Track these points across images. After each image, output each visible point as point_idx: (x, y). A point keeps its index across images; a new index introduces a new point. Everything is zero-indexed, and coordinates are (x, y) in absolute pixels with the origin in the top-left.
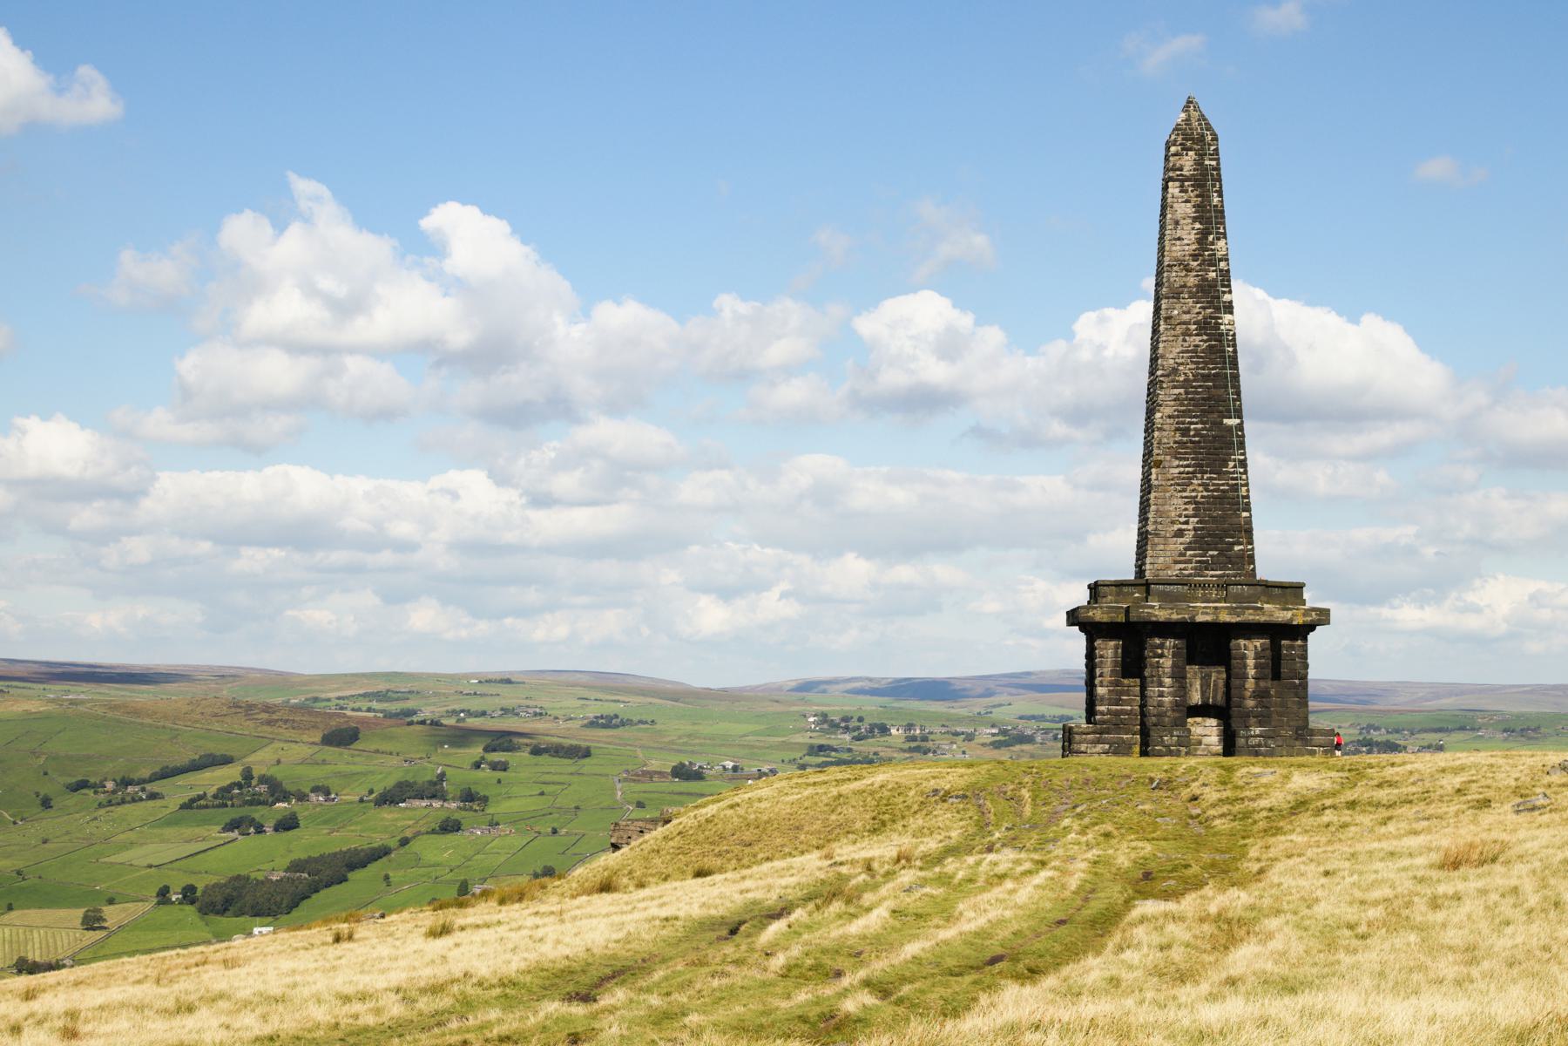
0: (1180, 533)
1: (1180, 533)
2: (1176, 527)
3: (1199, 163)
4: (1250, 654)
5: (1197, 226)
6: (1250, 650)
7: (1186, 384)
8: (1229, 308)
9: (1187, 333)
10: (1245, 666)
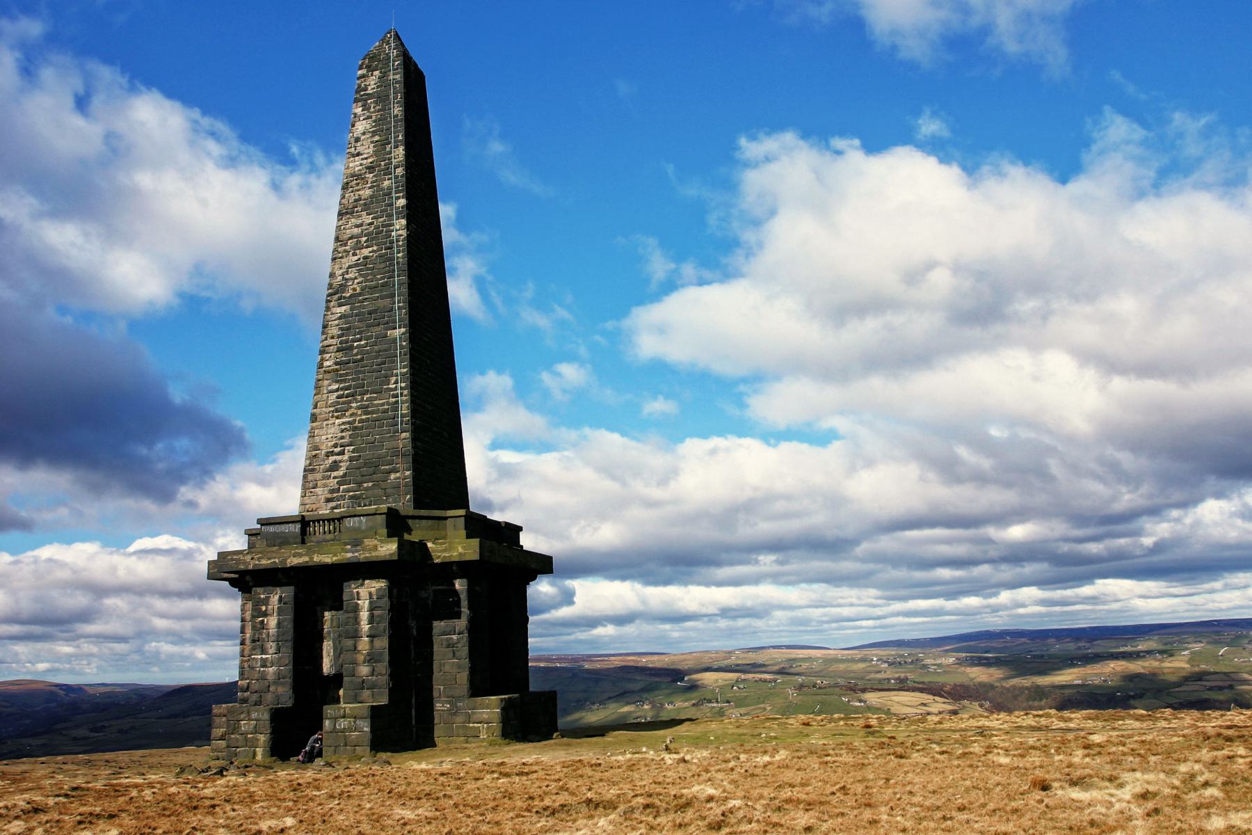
0: (335, 466)
1: (335, 466)
4: (364, 604)
10: (357, 620)
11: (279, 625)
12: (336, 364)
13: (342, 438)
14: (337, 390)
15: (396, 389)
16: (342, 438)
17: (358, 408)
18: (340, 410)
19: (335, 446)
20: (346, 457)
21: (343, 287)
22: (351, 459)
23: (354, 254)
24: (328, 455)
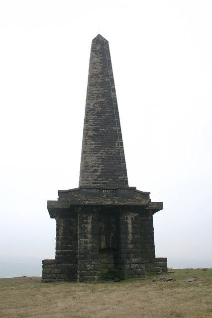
0: (96, 171)
1: (96, 171)
3: (102, 48)
4: (129, 221)
6: (129, 220)
7: (97, 114)
8: (114, 90)
9: (98, 97)
10: (127, 228)
11: (92, 228)
12: (93, 135)
13: (98, 161)
14: (94, 144)
16: (98, 161)
17: (104, 152)
18: (95, 151)
19: (95, 164)
20: (100, 168)
21: (93, 109)
22: (102, 169)
24: (92, 167)
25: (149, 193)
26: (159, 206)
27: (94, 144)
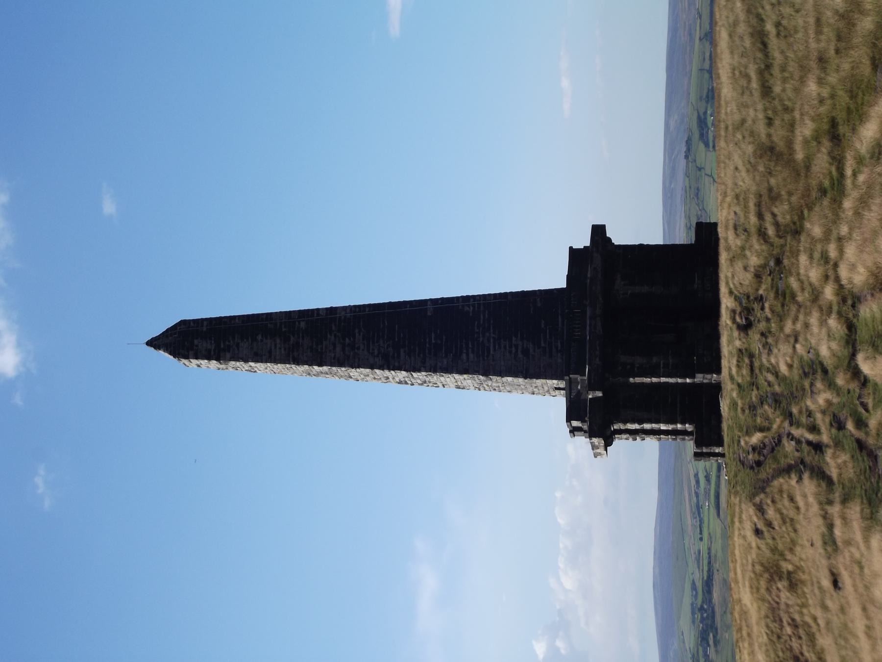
0: (526, 352)
1: (526, 352)
2: (520, 355)
5: (259, 337)
8: (332, 310)
13: (505, 347)
14: (467, 354)
15: (473, 306)
16: (505, 347)
19: (510, 352)
20: (520, 343)
23: (358, 348)
25: (571, 248)
26: (598, 231)
27: (467, 354)
